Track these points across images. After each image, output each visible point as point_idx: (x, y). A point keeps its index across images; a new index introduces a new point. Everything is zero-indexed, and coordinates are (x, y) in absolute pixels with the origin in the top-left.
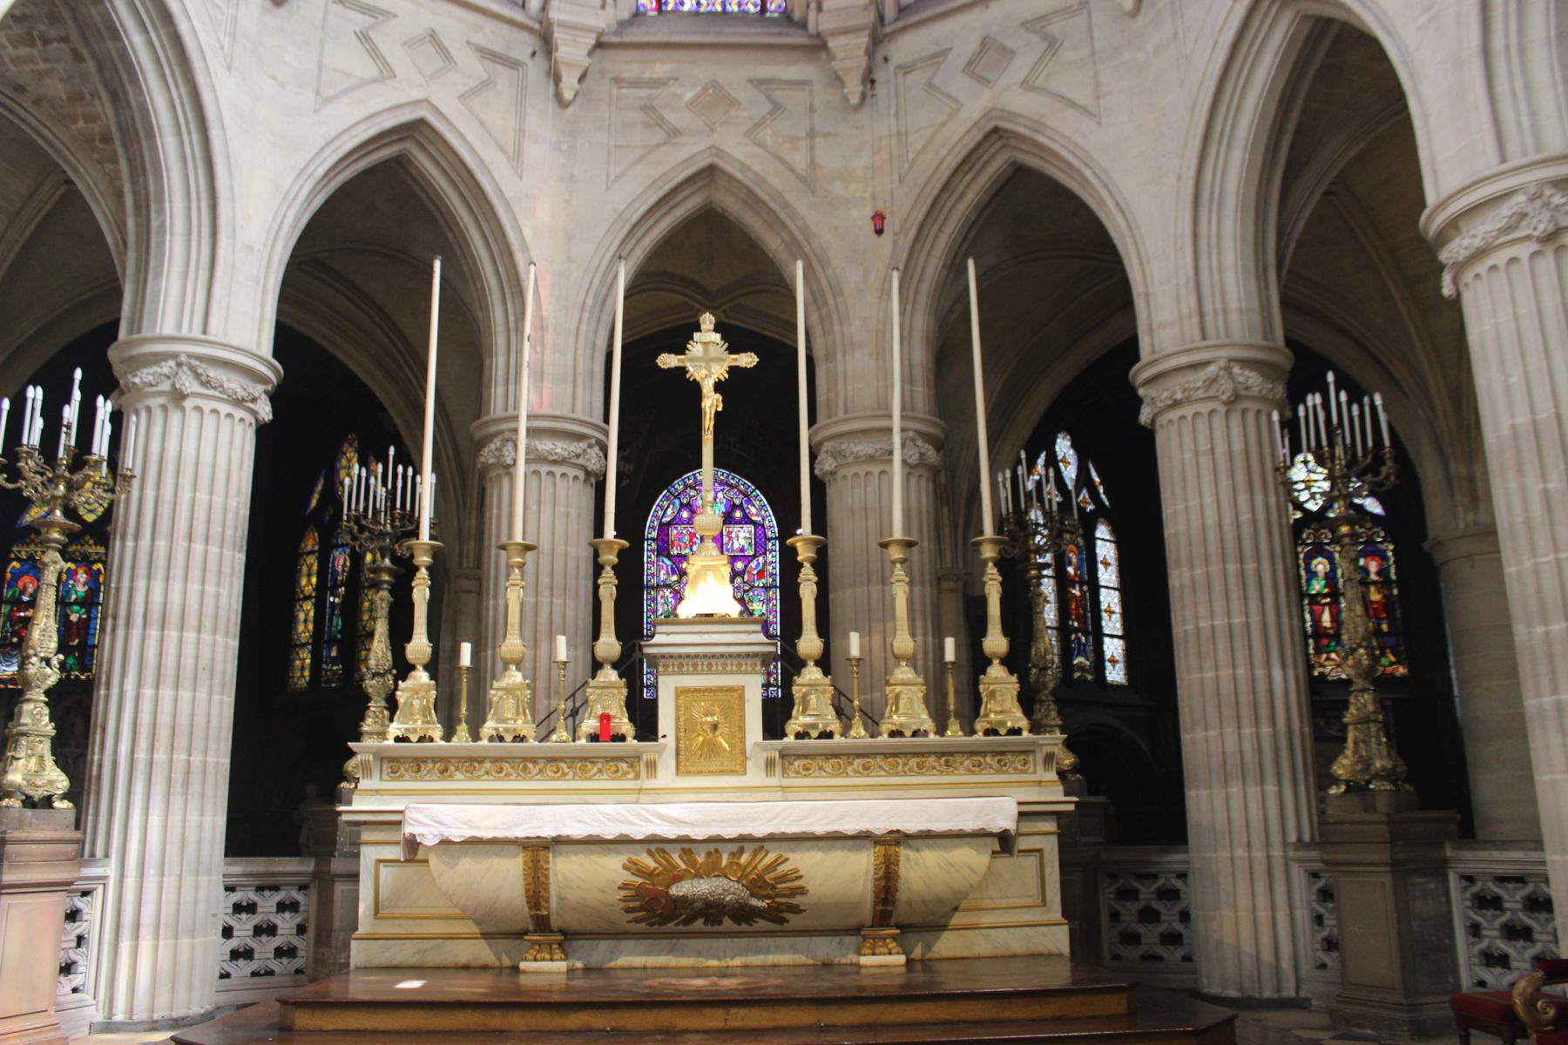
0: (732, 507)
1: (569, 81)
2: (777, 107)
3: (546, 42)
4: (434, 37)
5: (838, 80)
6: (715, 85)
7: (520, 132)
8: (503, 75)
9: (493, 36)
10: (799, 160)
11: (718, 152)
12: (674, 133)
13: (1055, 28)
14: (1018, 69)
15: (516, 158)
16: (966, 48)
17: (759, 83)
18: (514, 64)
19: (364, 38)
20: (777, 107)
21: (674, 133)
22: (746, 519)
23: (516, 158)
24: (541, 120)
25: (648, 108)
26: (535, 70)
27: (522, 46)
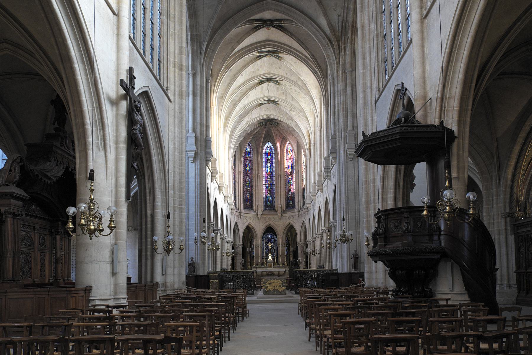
1: (259, 218)
3: (257, 215)
4: (250, 217)
5: (279, 217)
6: (270, 217)
9: (253, 216)
10: (276, 223)
13: (294, 216)
14: (291, 219)
15: (256, 225)
16: (288, 216)
17: (273, 217)
19: (246, 219)
21: (267, 222)
25: (265, 219)
26: (257, 217)
27: (256, 216)
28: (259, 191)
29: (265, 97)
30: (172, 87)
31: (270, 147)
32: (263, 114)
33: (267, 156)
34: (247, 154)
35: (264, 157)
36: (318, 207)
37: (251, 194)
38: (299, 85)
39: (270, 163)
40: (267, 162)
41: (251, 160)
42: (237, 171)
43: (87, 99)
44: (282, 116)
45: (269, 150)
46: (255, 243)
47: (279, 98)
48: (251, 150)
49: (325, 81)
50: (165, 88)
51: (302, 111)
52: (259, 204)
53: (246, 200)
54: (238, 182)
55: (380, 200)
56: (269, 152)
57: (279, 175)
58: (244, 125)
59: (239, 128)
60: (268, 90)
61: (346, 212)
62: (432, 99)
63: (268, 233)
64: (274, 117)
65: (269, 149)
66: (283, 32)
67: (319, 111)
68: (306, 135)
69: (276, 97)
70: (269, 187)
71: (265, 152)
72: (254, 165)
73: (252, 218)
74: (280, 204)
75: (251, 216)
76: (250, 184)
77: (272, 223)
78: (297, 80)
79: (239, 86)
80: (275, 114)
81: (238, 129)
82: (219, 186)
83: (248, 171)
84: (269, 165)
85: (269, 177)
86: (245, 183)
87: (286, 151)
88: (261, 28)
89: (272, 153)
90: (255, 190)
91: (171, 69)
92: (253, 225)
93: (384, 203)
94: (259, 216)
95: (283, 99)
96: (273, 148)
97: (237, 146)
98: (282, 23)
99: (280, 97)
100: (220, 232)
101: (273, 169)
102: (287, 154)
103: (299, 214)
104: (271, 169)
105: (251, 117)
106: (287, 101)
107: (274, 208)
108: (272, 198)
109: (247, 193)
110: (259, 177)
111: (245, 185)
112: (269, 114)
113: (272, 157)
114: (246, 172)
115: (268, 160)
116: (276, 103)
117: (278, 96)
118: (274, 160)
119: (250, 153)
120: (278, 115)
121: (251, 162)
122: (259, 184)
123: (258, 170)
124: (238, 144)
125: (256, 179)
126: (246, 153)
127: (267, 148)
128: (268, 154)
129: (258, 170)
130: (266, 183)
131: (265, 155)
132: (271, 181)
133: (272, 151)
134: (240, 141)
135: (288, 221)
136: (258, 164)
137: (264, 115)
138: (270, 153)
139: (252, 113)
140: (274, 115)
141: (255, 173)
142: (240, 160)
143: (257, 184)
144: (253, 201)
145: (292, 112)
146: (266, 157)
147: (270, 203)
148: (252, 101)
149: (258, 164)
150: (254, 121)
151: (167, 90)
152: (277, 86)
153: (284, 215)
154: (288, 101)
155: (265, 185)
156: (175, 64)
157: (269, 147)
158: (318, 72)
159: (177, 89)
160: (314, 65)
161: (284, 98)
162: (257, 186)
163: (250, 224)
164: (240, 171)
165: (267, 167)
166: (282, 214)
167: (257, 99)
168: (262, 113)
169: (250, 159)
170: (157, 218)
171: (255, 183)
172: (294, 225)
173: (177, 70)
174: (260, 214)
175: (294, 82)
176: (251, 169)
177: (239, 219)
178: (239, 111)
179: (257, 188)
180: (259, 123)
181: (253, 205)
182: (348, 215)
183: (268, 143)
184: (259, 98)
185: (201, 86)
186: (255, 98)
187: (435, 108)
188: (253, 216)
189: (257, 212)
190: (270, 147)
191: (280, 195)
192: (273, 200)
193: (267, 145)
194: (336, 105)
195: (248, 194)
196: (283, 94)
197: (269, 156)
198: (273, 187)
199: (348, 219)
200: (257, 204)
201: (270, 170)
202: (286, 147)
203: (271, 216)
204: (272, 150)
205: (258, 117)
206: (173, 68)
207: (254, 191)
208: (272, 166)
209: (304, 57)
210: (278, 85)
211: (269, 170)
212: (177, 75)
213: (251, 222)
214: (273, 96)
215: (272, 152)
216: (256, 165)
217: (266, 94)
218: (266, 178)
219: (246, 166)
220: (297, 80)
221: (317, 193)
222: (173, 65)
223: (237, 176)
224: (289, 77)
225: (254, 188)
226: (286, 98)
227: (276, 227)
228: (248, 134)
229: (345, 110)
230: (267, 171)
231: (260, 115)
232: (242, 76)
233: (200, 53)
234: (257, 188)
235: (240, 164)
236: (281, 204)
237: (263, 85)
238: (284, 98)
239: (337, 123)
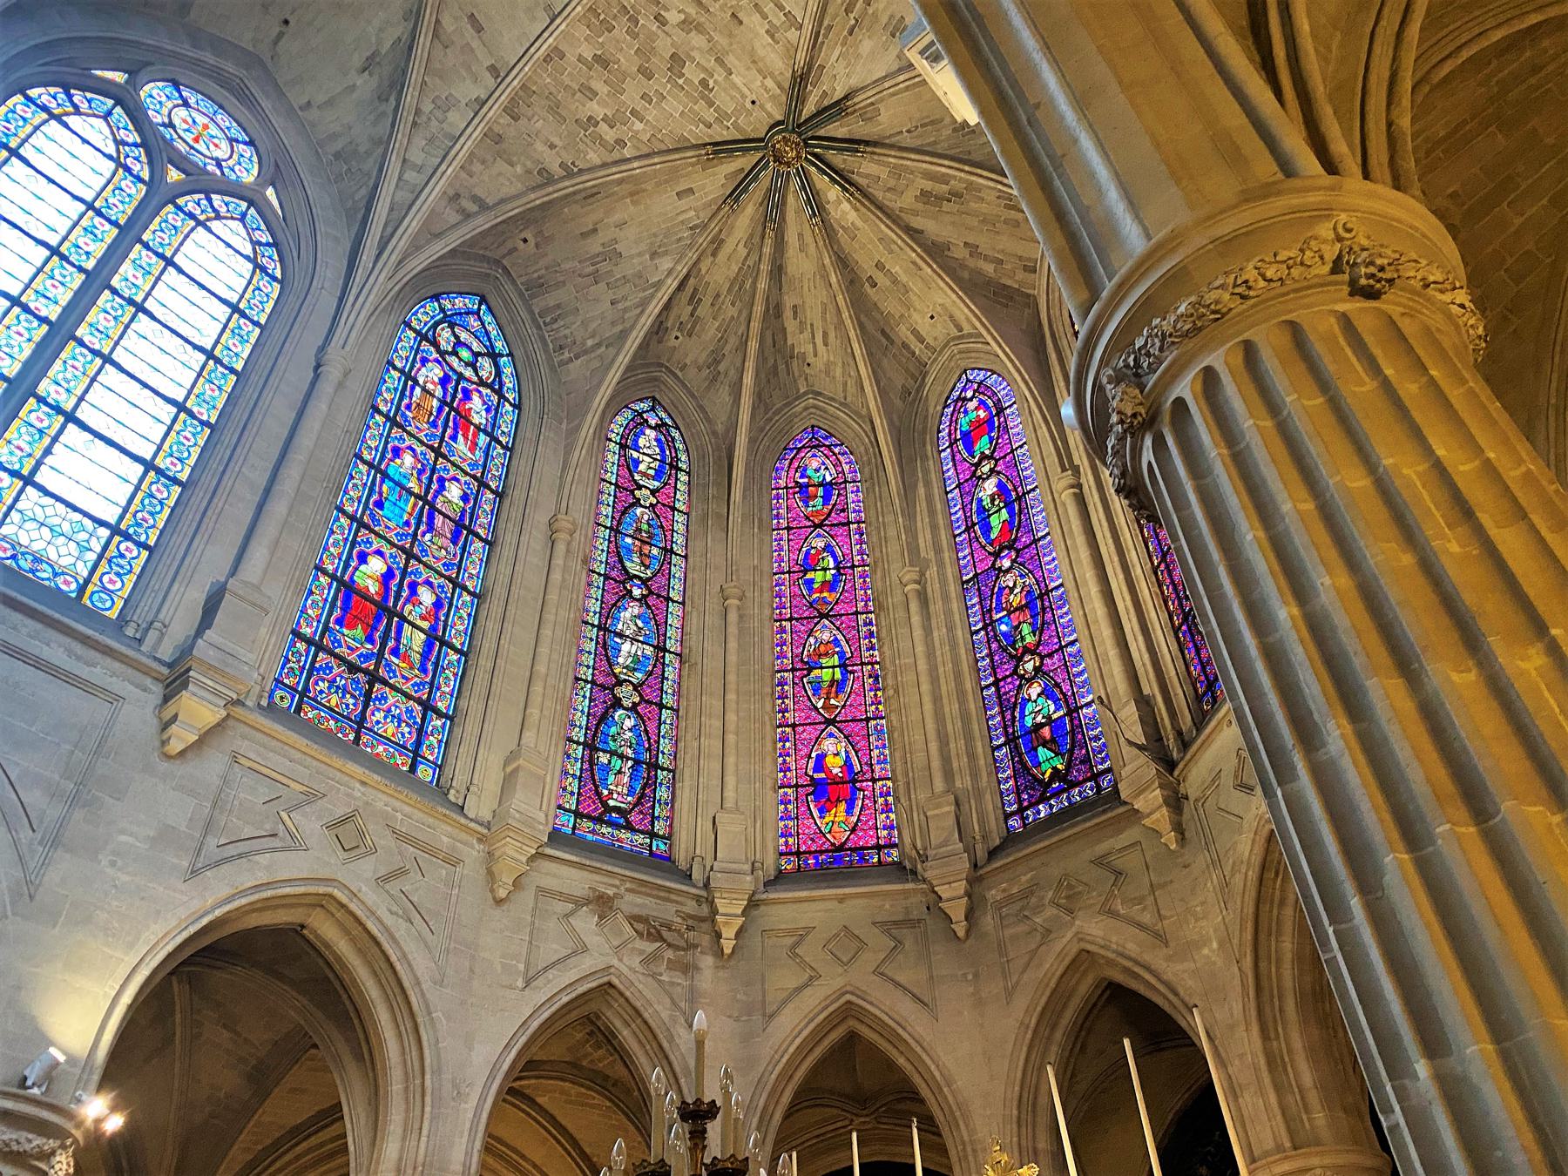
8: (908, 937)
10: (1147, 918)
17: (1100, 862)
73: (880, 942)
77: (1094, 929)
132: (1030, 580)
147: (1053, 744)
153: (1196, 776)
177: (688, 969)
188: (889, 909)
192: (1073, 711)
197: (983, 445)
201: (1004, 514)
227: (1157, 959)
230: (987, 528)
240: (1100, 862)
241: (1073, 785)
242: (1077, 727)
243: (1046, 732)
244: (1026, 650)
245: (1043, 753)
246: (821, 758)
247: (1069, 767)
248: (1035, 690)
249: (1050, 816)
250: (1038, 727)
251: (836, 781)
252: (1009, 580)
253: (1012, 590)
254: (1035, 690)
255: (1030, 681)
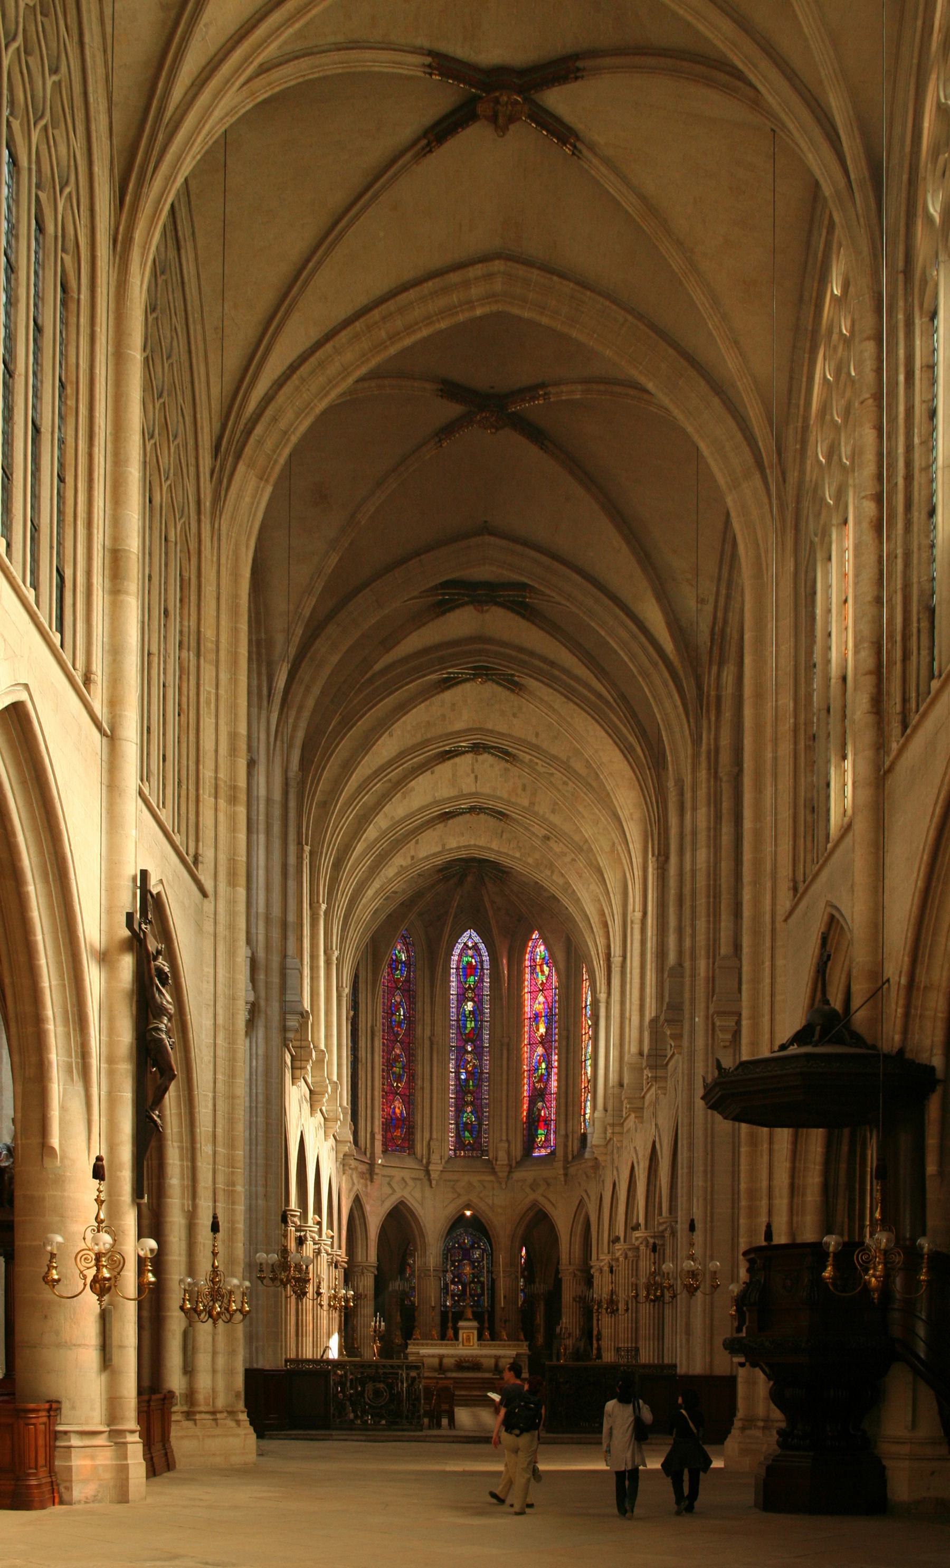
0: (474, 1243)
1: (434, 1182)
2: (485, 1187)
3: (428, 1172)
4: (403, 1179)
7: (423, 1197)
8: (418, 1182)
9: (415, 1174)
11: (470, 1200)
12: (459, 1195)
15: (422, 1204)
17: (480, 1181)
18: (421, 1179)
20: (485, 1187)
21: (459, 1195)
22: (479, 1247)
23: (422, 1204)
24: (428, 1193)
25: (453, 1188)
27: (422, 1174)
28: (435, 1095)
29: (465, 795)
30: (207, 854)
31: (475, 947)
32: (454, 845)
33: (466, 976)
34: (397, 969)
35: (453, 978)
36: (629, 1164)
37: (409, 1102)
38: (575, 771)
39: (472, 1000)
40: (462, 998)
41: (409, 991)
42: (362, 1026)
43: (50, 961)
44: (518, 855)
45: (472, 957)
46: (416, 1262)
47: (509, 802)
48: (408, 957)
49: (659, 777)
50: (190, 860)
51: (585, 848)
52: (434, 1136)
53: (390, 1123)
54: (364, 1061)
55: (785, 1191)
56: (469, 963)
57: (502, 1045)
58: (391, 881)
59: (374, 890)
60: (472, 776)
61: (705, 1199)
62: (891, 980)
63: (462, 1230)
64: (492, 857)
65: (470, 952)
66: (528, 620)
67: (640, 860)
68: (597, 920)
69: (500, 798)
70: (466, 1080)
71: (459, 961)
72: (419, 1005)
73: (411, 1183)
74: (504, 1138)
75: (406, 1174)
76: (403, 1068)
78: (569, 758)
79: (382, 766)
80: (494, 846)
81: (370, 893)
82: (310, 1091)
83: (400, 1024)
84: (470, 1006)
85: (469, 1049)
86: (389, 1063)
87: (527, 963)
88: (457, 607)
89: (482, 969)
90: (423, 1088)
91: (207, 800)
92: (413, 1203)
93: (795, 1200)
94: (434, 1175)
95: (524, 807)
96: (484, 952)
97: (362, 947)
98: (525, 597)
99: (513, 800)
100: (314, 1235)
101: (482, 1021)
102: (532, 973)
103: (566, 1175)
104: (476, 1021)
105: (412, 853)
106: (535, 814)
107: (483, 1151)
108: (479, 1119)
109: (393, 1101)
110: (435, 1047)
111: (388, 1073)
112: (475, 845)
113: (481, 980)
114: (393, 1029)
115: (467, 990)
116: (501, 816)
117: (505, 796)
118: (486, 992)
119: (407, 964)
120: (505, 851)
121: (410, 995)
122: (435, 1069)
123: (433, 1024)
124: (367, 939)
125: (427, 1054)
126: (395, 963)
127: (463, 949)
128: (469, 970)
129: (433, 1024)
130: (458, 1067)
131: (458, 975)
132: (477, 1062)
133: (482, 962)
134: (374, 928)
135: (532, 1196)
136: (432, 1003)
137: (459, 848)
138: (475, 968)
139: (417, 842)
140: (489, 849)
141: (423, 1032)
142: (373, 995)
143: (427, 1069)
144: (413, 1128)
145: (552, 844)
146: (459, 981)
147: (471, 1133)
148: (419, 809)
149: (432, 1003)
150: (427, 865)
151: (196, 861)
152: (504, 764)
154: (541, 813)
155: (458, 1074)
156: (216, 787)
157: (470, 945)
158: (639, 750)
159: (222, 857)
160: (625, 726)
161: (526, 803)
162: (427, 1076)
163: (402, 1203)
164: (372, 1027)
165: (465, 1016)
166: (510, 1172)
167: (436, 803)
168: (453, 843)
169: (406, 987)
170: (169, 1219)
171: (421, 1068)
172: (549, 1209)
173: (222, 803)
174: (436, 1168)
175: (563, 762)
176: (410, 1020)
178: (377, 840)
179: (427, 1085)
180: (440, 871)
181: (413, 1140)
182: (712, 1208)
183: (467, 934)
184: (444, 800)
185: (269, 801)
186: (429, 799)
187: (895, 1008)
188: (415, 1174)
189: (428, 1163)
190: (475, 947)
191: (504, 1109)
192: (480, 1124)
193: (464, 939)
194: (688, 877)
195: (397, 1103)
196: (524, 789)
198: (481, 1080)
199: (712, 1222)
200: (427, 1136)
201: (473, 1025)
202: (529, 949)
203: (475, 1179)
204: (480, 955)
205: (439, 852)
206: (213, 800)
207: (418, 1094)
208: (482, 1013)
209: (593, 698)
210: (507, 761)
211: (470, 1025)
212: (222, 817)
213: (406, 1194)
214: (489, 795)
215: (482, 966)
216: (427, 1008)
217: (468, 785)
218: (461, 1051)
219: (390, 1011)
220: (569, 758)
221: (626, 1118)
222: (213, 791)
223: (362, 1043)
224: (545, 745)
225: (419, 1082)
226: (532, 804)
228: (402, 904)
229: (714, 894)
230: (466, 1027)
231: (444, 846)
232: (391, 735)
233: (269, 696)
234: (427, 1085)
235: (373, 1001)
236: (508, 1141)
237: (457, 760)
238: (526, 803)
239: (688, 930)
240: (480, 1181)
241: (473, 1150)
242: (480, 1131)
243: (469, 1126)
244: (470, 1092)
245: (467, 1134)
246: (394, 1108)
247: (474, 1142)
248: (469, 1109)
249: (464, 1156)
250: (466, 1124)
251: (397, 1119)
252: (469, 1057)
253: (469, 1063)
254: (469, 1109)
255: (468, 1104)
